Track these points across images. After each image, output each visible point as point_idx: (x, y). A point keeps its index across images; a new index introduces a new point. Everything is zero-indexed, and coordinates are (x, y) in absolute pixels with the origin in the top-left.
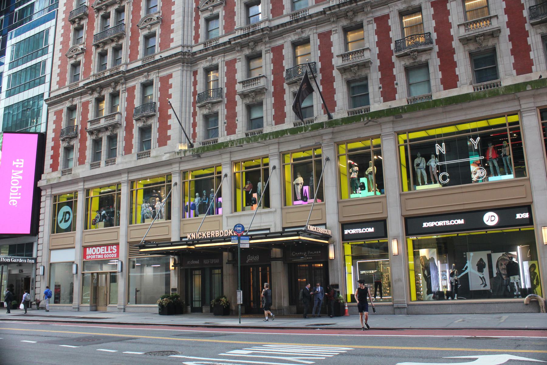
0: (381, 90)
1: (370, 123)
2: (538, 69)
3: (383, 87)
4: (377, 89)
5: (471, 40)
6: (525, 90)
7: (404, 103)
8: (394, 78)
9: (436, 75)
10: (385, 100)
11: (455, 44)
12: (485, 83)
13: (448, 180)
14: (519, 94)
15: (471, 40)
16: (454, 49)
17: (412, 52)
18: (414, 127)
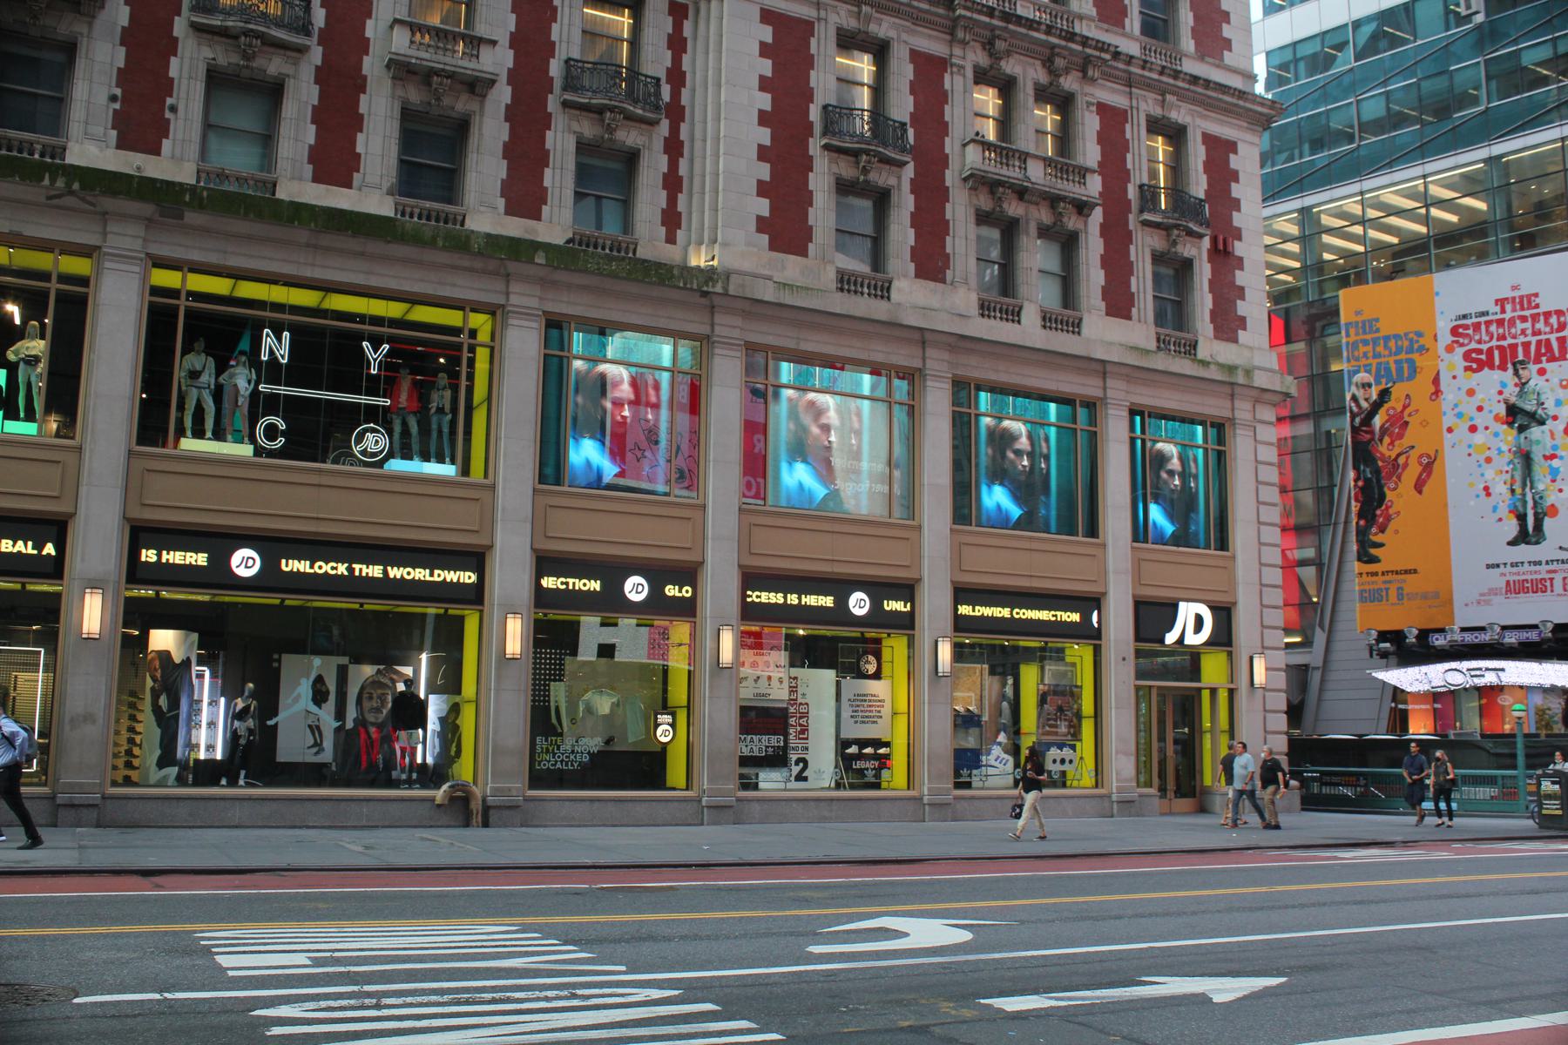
0: (117, 106)
1: (69, 201)
2: (555, 219)
3: (125, 100)
4: (102, 98)
5: (415, 73)
6: (531, 261)
7: (185, 174)
8: (167, 86)
9: (297, 133)
10: (122, 144)
11: (371, 66)
12: (428, 204)
13: (281, 441)
14: (512, 266)
15: (415, 73)
16: (365, 78)
17: (247, 33)
18: (213, 258)
